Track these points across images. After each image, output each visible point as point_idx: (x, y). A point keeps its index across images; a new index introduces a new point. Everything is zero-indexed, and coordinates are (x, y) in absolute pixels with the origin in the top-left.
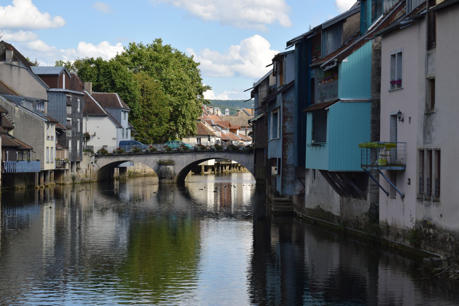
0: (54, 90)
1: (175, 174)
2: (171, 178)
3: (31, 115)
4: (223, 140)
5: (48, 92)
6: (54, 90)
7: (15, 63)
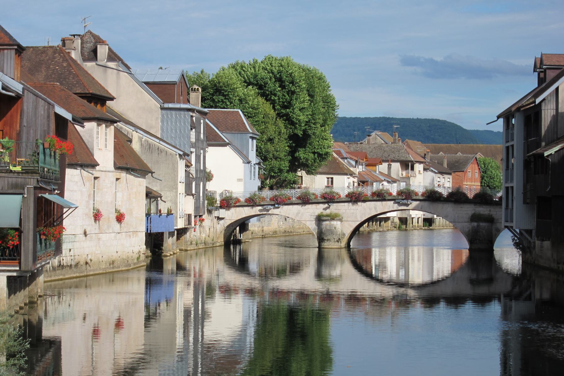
0: (171, 105)
1: (344, 235)
2: (339, 241)
3: (157, 144)
4: (360, 181)
5: (162, 109)
6: (171, 105)
7: (112, 64)
